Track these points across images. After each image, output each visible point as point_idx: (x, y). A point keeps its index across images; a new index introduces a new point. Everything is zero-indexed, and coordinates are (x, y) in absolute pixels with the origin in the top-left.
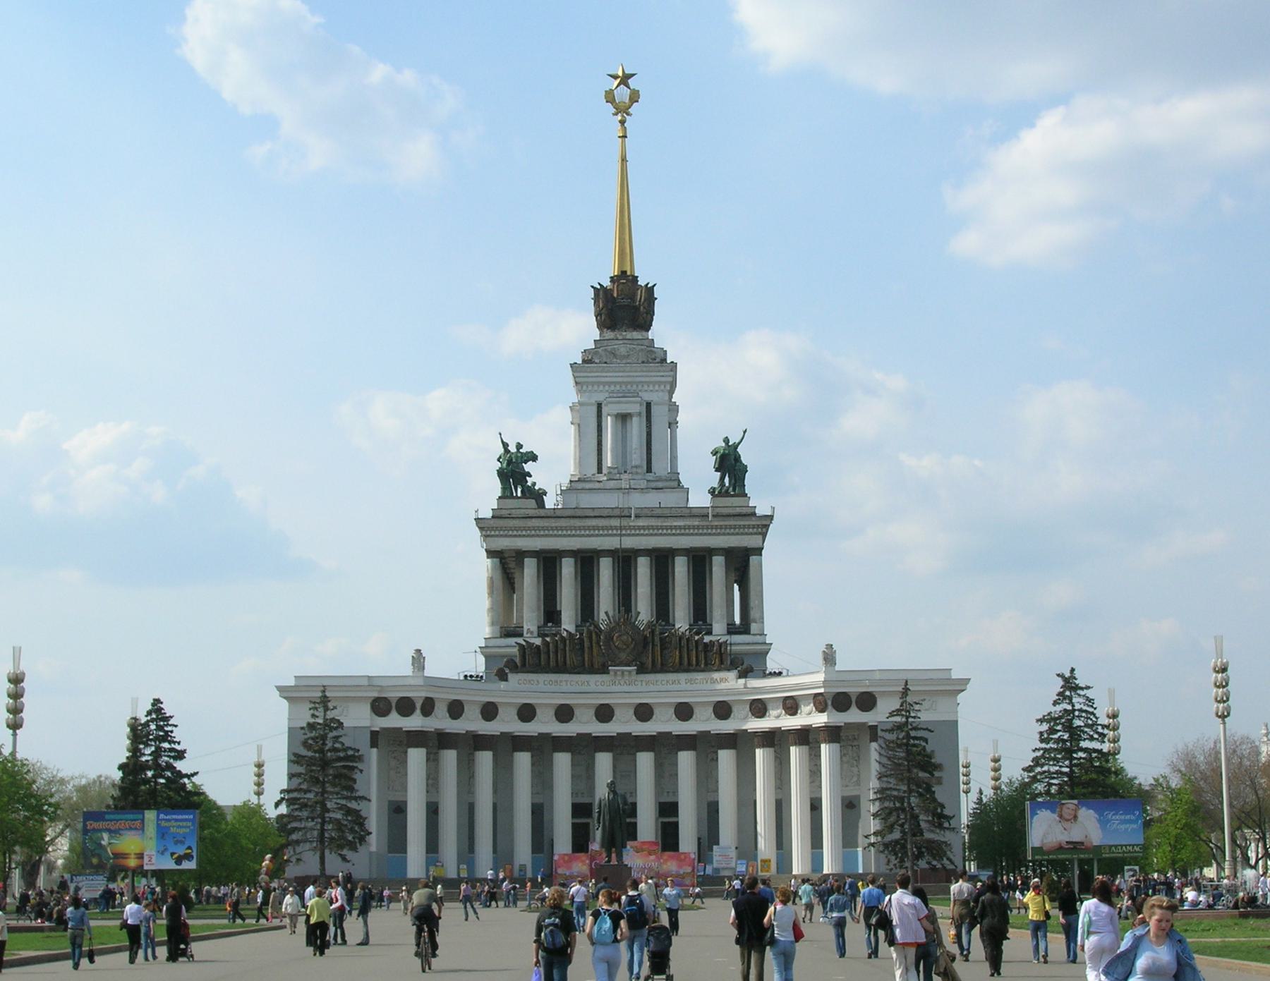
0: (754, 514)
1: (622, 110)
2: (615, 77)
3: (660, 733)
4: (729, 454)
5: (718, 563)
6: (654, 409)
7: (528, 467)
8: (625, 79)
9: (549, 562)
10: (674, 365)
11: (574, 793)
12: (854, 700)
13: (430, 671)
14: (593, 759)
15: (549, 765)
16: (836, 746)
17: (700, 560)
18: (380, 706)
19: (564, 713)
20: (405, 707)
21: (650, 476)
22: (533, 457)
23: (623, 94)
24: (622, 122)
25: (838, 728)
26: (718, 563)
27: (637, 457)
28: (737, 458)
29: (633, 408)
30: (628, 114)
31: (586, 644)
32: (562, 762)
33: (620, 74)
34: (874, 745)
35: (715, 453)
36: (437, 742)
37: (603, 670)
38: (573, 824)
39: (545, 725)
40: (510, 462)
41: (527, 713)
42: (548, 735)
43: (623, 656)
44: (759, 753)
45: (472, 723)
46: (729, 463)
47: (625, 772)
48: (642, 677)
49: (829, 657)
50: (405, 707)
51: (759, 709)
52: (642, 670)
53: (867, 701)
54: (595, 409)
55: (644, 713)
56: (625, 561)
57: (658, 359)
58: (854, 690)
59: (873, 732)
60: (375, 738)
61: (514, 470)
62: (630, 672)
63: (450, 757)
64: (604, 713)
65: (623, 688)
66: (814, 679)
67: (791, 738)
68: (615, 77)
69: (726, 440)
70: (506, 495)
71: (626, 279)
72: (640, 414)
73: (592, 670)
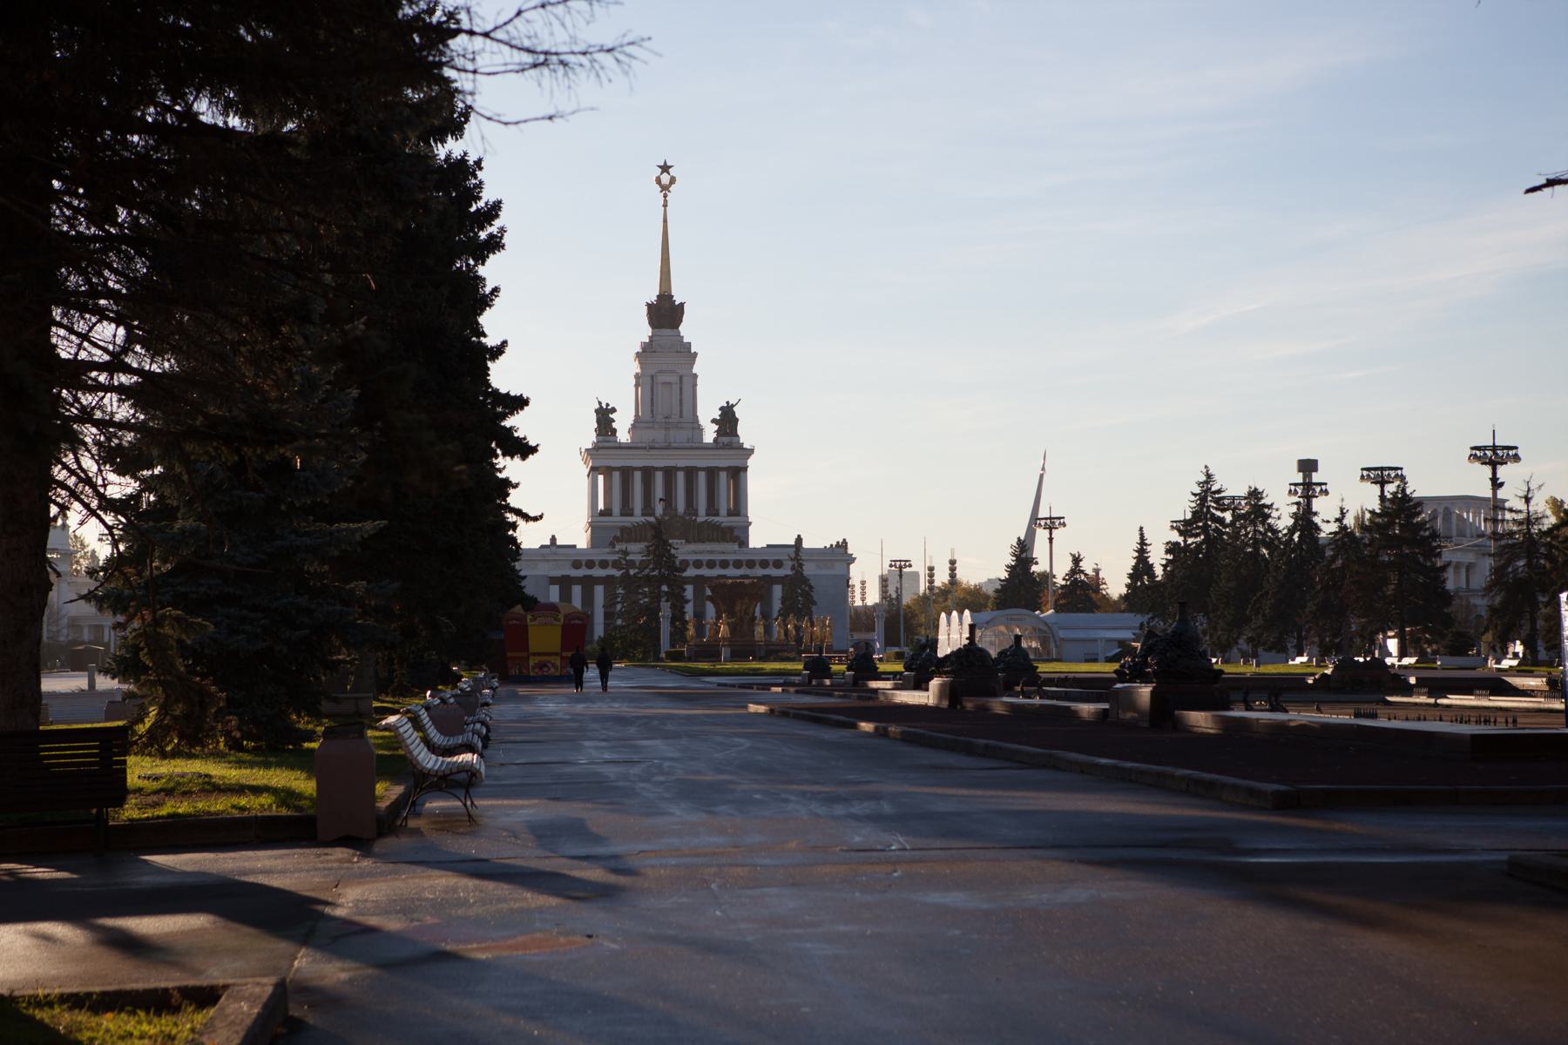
0: (741, 447)
1: (665, 189)
5: (723, 475)
6: (685, 380)
8: (665, 168)
9: (626, 473)
10: (695, 354)
17: (712, 473)
22: (614, 410)
23: (665, 179)
26: (723, 475)
27: (676, 410)
52: (688, 542)
56: (669, 473)
61: (604, 416)
71: (665, 297)
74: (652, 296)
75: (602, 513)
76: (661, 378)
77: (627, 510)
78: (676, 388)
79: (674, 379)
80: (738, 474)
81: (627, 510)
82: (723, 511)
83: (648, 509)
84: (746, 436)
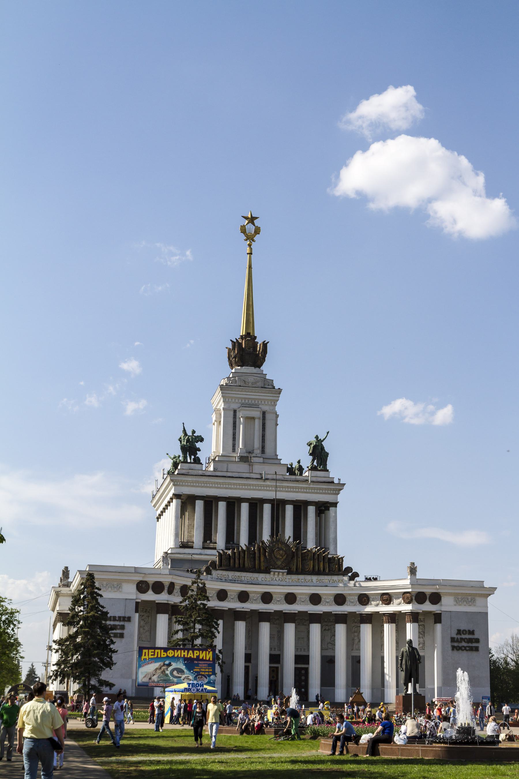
0: (333, 482)
1: (250, 238)
2: (246, 218)
3: (299, 612)
4: (318, 446)
5: (311, 510)
6: (268, 416)
7: (198, 445)
8: (252, 220)
9: (210, 503)
10: (280, 391)
11: (296, 649)
12: (428, 597)
14: (334, 628)
15: (233, 629)
16: (416, 625)
17: (300, 507)
18: (142, 587)
19: (243, 597)
20: (158, 587)
21: (264, 455)
22: (201, 439)
23: (251, 229)
24: (250, 245)
25: (418, 614)
26: (311, 510)
28: (323, 448)
30: (253, 241)
31: (257, 555)
33: (250, 216)
34: (439, 626)
35: (309, 444)
37: (267, 571)
38: (270, 667)
40: (188, 441)
42: (281, 611)
43: (279, 563)
44: (386, 626)
48: (289, 576)
49: (413, 570)
50: (158, 587)
51: (364, 599)
52: (290, 573)
53: (436, 598)
54: (232, 413)
55: (291, 598)
56: (255, 505)
57: (268, 386)
58: (428, 590)
59: (437, 618)
60: (139, 606)
61: (190, 446)
62: (283, 573)
64: (267, 598)
65: (278, 584)
66: (405, 583)
67: (407, 618)
68: (246, 218)
69: (317, 437)
71: (249, 336)
72: (259, 418)
73: (260, 571)
75: (184, 546)
78: (258, 424)
79: (256, 413)
84: (335, 469)
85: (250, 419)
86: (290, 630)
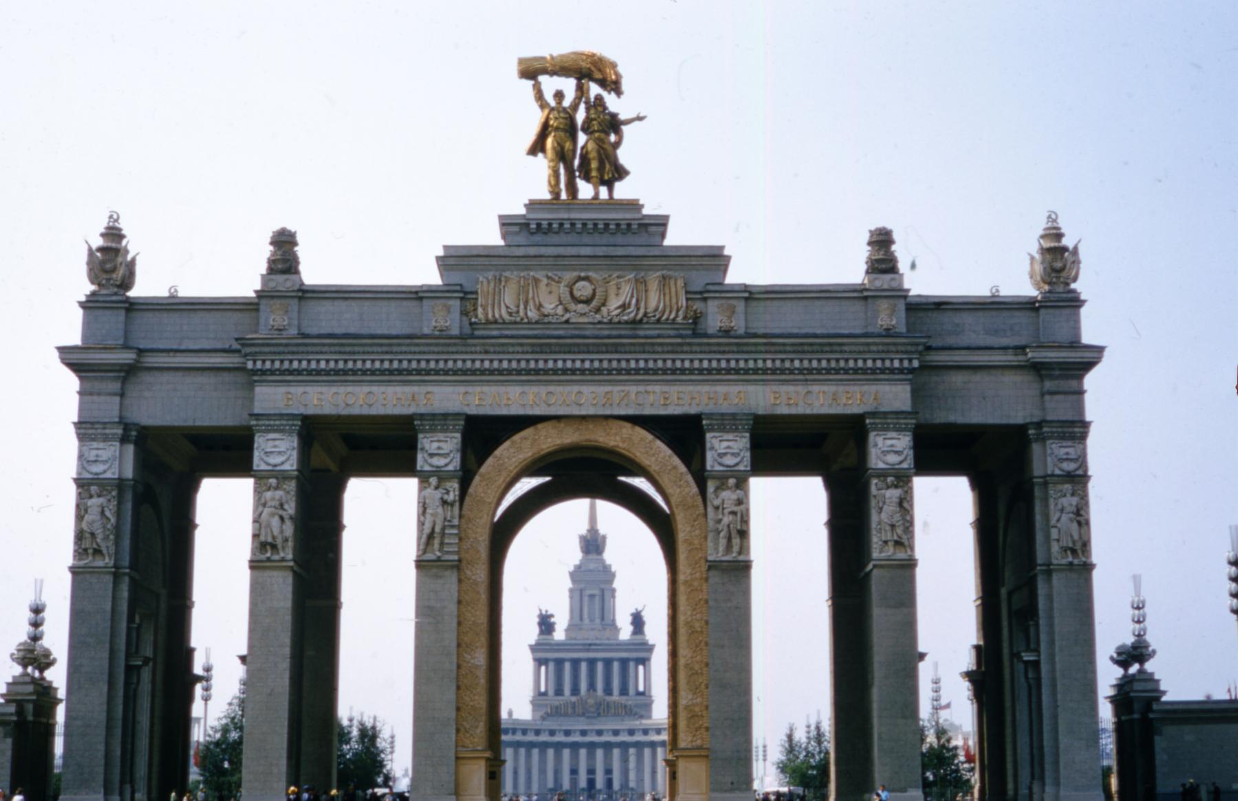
5: (632, 664)
9: (559, 663)
13: (515, 716)
17: (624, 663)
27: (597, 614)
29: (596, 592)
32: (566, 753)
36: (517, 745)
39: (560, 738)
41: (552, 733)
45: (531, 737)
46: (638, 622)
47: (591, 756)
51: (646, 732)
63: (522, 751)
70: (542, 632)
71: (593, 530)
74: (583, 529)
75: (541, 694)
76: (588, 592)
77: (559, 692)
78: (597, 600)
79: (596, 592)
80: (644, 661)
81: (559, 692)
82: (632, 691)
83: (575, 690)
85: (592, 596)
86: (616, 752)
